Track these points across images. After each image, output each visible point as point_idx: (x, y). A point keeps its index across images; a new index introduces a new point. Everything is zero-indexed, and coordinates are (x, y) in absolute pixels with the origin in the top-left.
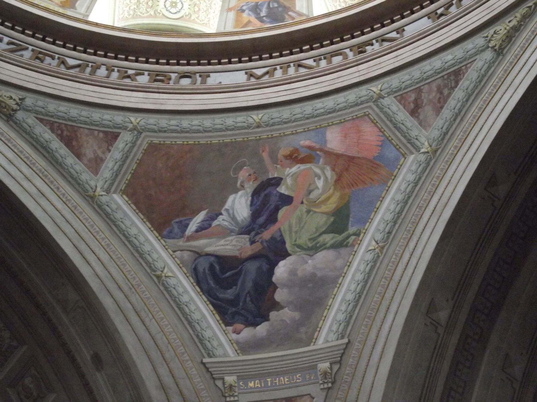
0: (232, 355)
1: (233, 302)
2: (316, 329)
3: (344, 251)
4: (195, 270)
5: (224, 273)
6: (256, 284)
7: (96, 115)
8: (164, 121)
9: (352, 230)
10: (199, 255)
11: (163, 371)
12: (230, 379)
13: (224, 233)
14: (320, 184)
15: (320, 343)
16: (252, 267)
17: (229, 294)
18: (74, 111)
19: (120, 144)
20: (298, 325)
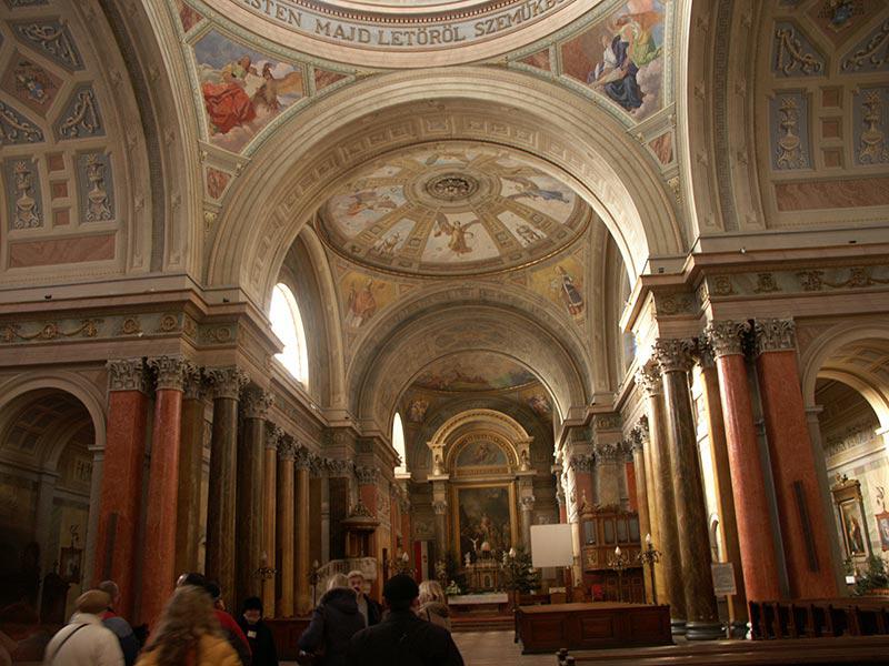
0: (637, 124)
1: (627, 100)
2: (662, 100)
3: (659, 59)
4: (607, 93)
5: (617, 87)
6: (632, 88)
7: (536, 46)
8: (561, 33)
9: (658, 48)
10: (605, 85)
11: (614, 152)
12: (639, 135)
13: (610, 71)
14: (636, 31)
15: (666, 107)
16: (627, 81)
17: (624, 97)
18: (527, 50)
19: (551, 53)
20: (654, 100)
